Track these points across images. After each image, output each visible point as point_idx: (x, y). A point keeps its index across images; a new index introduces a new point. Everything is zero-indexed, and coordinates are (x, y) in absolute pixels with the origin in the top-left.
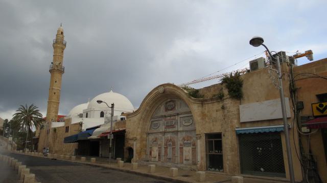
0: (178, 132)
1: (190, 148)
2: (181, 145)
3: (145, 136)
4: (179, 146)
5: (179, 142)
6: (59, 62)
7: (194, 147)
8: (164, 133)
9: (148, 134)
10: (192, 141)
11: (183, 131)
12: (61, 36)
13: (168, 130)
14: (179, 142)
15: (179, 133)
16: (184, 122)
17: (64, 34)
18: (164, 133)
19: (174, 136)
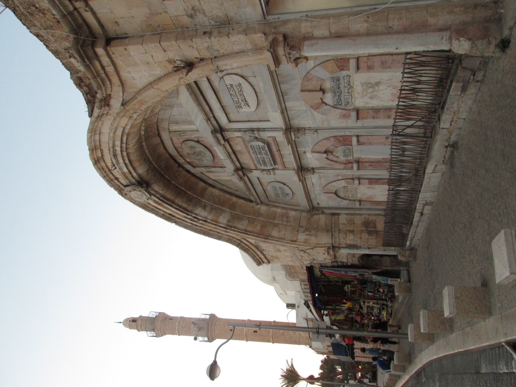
0: (289, 129)
1: (359, 79)
2: (345, 117)
3: (322, 219)
4: (351, 122)
5: (334, 120)
6: (192, 326)
7: (352, 63)
8: (302, 170)
9: (314, 209)
10: (322, 73)
11: (284, 111)
12: (139, 322)
13: (290, 160)
14: (334, 120)
15: (296, 123)
16: (245, 109)
17: (136, 315)
18: (302, 170)
19: (308, 141)
